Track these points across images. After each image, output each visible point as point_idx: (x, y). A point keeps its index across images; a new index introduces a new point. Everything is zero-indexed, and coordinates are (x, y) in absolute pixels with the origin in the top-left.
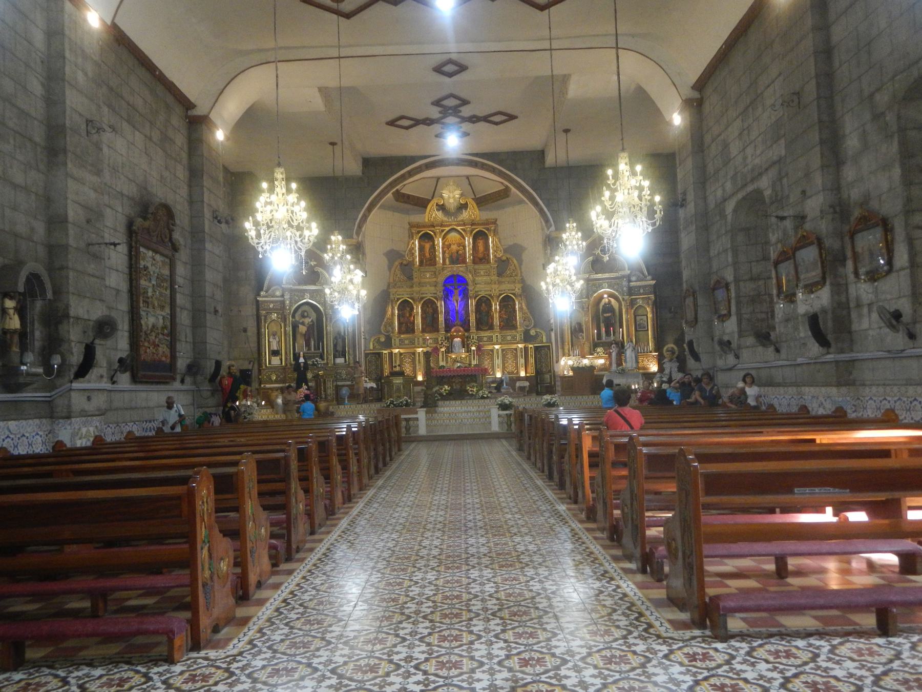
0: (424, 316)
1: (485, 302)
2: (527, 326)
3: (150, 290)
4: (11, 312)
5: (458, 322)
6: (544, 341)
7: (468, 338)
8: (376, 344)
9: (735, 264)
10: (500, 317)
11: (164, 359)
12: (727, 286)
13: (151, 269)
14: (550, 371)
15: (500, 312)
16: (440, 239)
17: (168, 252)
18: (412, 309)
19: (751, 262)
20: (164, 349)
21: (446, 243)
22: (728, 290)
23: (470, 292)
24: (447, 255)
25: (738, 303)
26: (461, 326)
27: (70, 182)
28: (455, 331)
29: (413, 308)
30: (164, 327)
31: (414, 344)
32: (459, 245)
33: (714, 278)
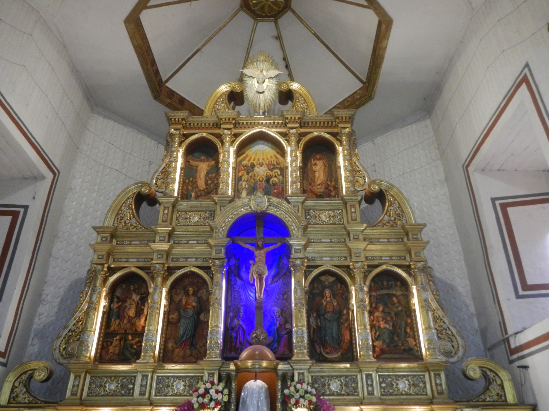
0: (174, 316)
1: (331, 287)
2: (448, 354)
5: (259, 333)
7: (286, 378)
8: (22, 389)
10: (372, 327)
15: (371, 313)
16: (232, 150)
18: (144, 298)
21: (244, 163)
23: (294, 255)
24: (244, 184)
26: (269, 346)
28: (251, 357)
29: (148, 293)
31: (130, 393)
32: (272, 167)
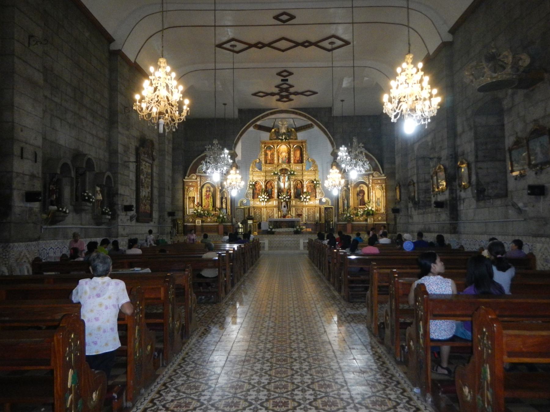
3: (144, 180)
4: (99, 192)
6: (330, 204)
9: (417, 174)
11: (148, 211)
12: (414, 183)
13: (145, 170)
14: (332, 221)
17: (151, 162)
19: (425, 174)
20: (148, 207)
22: (414, 186)
25: (418, 193)
27: (119, 135)
30: (148, 197)
33: (409, 180)
